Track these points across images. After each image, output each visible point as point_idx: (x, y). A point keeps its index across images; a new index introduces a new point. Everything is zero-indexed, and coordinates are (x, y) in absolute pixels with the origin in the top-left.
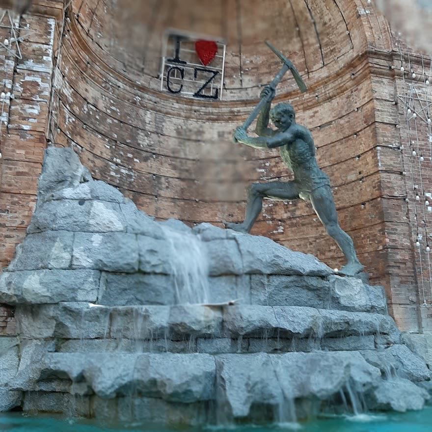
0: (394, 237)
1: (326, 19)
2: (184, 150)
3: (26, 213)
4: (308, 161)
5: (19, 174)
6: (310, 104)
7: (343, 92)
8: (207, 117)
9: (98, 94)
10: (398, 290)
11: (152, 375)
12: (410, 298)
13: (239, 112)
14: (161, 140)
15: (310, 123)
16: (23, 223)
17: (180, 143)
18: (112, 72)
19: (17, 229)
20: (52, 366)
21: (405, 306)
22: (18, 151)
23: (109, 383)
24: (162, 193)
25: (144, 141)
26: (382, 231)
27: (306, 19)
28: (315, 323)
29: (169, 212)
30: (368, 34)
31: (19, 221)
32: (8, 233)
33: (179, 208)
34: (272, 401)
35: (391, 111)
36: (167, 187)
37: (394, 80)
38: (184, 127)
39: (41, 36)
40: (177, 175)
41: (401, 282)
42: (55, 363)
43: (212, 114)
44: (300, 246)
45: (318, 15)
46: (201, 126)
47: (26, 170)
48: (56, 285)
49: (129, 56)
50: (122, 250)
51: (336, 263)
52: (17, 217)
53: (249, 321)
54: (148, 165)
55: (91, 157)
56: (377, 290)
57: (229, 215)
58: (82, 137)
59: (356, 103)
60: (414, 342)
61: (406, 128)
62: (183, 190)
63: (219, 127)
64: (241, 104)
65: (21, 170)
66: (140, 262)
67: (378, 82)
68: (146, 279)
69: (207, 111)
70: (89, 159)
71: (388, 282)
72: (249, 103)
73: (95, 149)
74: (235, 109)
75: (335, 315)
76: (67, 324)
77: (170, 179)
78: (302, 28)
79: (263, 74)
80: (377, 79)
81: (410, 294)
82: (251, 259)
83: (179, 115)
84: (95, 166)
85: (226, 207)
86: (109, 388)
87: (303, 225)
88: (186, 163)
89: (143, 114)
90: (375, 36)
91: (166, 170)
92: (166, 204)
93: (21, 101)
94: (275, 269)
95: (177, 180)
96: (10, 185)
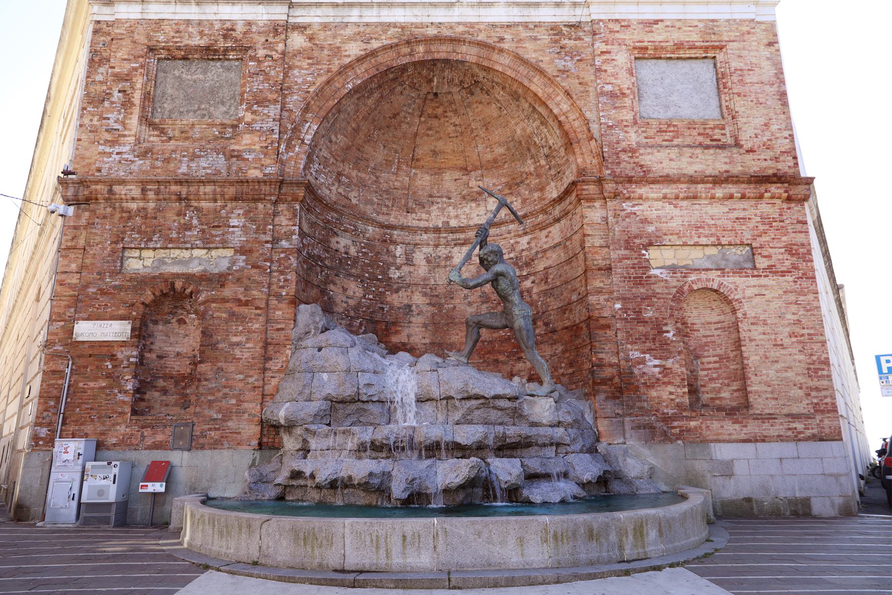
0: (601, 356)
1: (551, 142)
2: (434, 278)
4: (510, 295)
5: (278, 330)
6: (544, 224)
7: (567, 214)
9: (349, 242)
12: (617, 411)
14: (412, 270)
15: (546, 243)
16: (282, 366)
17: (430, 270)
19: (279, 371)
20: (296, 468)
22: (277, 313)
23: (324, 478)
24: (413, 319)
25: (394, 274)
27: (535, 143)
31: (280, 365)
32: (272, 375)
34: (428, 492)
35: (602, 234)
36: (418, 314)
38: (433, 255)
39: (290, 219)
40: (428, 301)
41: (607, 398)
43: (459, 239)
45: (544, 140)
46: (450, 252)
47: (282, 326)
55: (344, 299)
58: (335, 284)
61: (617, 249)
62: (433, 315)
65: (279, 326)
67: (589, 207)
68: (365, 406)
78: (533, 150)
79: (505, 195)
80: (588, 204)
82: (446, 387)
83: (428, 244)
84: (348, 306)
88: (436, 288)
89: (393, 250)
91: (418, 299)
92: (417, 329)
94: (466, 395)
96: (272, 339)
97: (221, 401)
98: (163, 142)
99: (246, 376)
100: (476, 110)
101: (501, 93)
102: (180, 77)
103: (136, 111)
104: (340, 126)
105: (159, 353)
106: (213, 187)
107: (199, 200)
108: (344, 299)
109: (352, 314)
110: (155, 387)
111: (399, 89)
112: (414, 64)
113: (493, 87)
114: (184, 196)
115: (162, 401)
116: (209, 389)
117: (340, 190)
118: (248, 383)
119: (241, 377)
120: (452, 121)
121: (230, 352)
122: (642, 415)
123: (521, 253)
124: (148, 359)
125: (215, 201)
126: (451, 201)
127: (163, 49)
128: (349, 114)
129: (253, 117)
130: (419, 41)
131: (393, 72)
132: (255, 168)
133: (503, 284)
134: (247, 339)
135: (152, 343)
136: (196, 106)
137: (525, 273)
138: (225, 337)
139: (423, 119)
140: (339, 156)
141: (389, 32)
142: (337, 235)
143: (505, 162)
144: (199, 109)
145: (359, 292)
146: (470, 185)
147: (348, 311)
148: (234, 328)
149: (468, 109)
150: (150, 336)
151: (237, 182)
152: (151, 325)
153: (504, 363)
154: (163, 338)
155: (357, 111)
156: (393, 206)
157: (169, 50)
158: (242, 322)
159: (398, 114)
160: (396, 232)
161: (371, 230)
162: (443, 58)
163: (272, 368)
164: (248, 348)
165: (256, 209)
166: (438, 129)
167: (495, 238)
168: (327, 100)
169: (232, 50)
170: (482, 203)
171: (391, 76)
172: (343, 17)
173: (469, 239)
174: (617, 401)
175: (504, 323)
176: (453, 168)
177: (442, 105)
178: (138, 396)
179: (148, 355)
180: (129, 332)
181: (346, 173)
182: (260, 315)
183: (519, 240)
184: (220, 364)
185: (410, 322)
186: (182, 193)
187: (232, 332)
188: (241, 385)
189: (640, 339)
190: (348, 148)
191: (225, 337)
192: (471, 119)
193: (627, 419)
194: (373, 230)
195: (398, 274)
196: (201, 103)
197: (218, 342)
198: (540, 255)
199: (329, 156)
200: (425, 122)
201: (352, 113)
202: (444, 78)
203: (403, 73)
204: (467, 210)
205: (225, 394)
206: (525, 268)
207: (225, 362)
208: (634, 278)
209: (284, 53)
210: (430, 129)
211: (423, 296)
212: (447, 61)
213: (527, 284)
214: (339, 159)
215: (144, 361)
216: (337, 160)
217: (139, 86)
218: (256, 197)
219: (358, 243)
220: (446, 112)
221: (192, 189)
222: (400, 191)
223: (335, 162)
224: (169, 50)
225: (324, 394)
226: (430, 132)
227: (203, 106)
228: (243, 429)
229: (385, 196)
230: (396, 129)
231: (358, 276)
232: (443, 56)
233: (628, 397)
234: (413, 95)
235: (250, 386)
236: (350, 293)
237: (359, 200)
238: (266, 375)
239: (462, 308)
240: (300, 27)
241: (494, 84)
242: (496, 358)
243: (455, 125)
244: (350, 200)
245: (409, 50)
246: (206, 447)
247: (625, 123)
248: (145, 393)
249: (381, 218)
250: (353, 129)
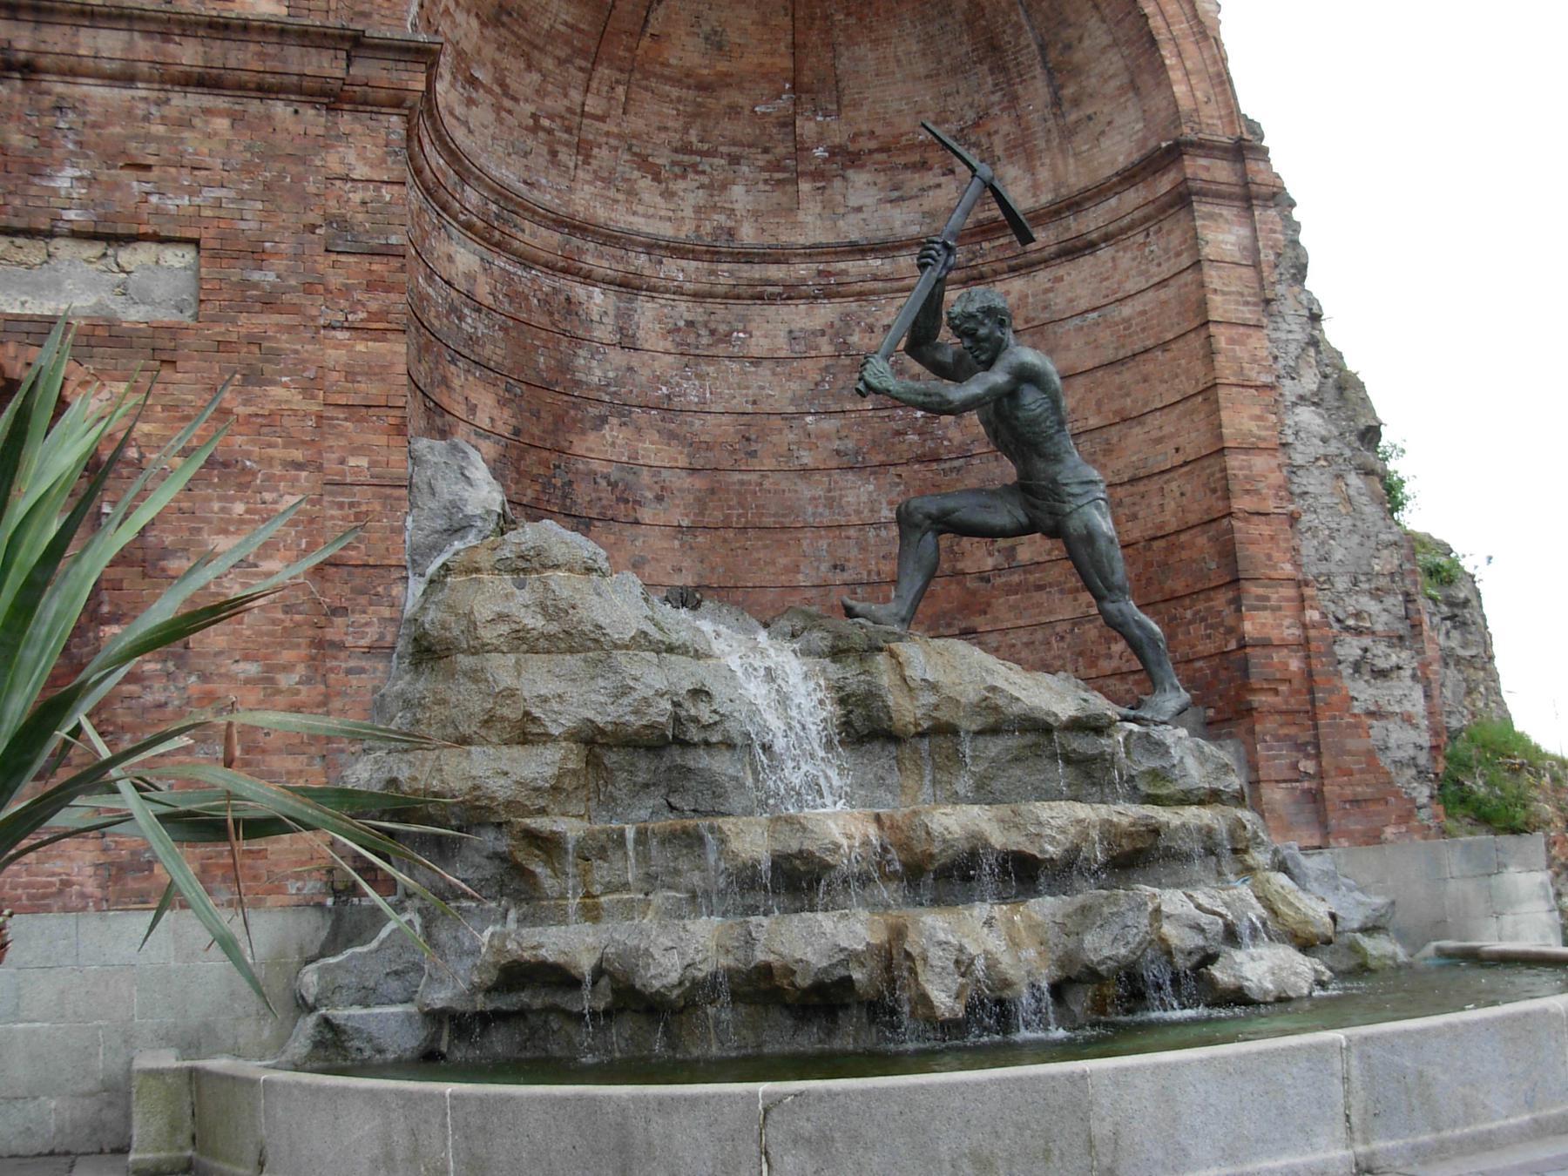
3: (386, 612)
11: (761, 956)
13: (844, 272)
16: (382, 637)
19: (371, 650)
20: (527, 955)
21: (1289, 785)
22: (352, 462)
24: (646, 514)
26: (1236, 602)
28: (1085, 836)
29: (669, 568)
30: (1180, 90)
32: (352, 663)
36: (659, 499)
37: (1250, 208)
40: (682, 461)
42: (533, 948)
44: (1032, 647)
48: (502, 782)
50: (635, 695)
51: (1127, 687)
52: (366, 624)
53: (944, 841)
56: (1224, 753)
57: (835, 567)
59: (1159, 265)
66: (677, 719)
71: (1252, 732)
72: (872, 250)
75: (1126, 813)
76: (532, 867)
77: (665, 474)
82: (933, 699)
86: (674, 986)
87: (1040, 588)
89: (583, 298)
90: (1199, 94)
93: (346, 335)
95: (684, 474)
99: (270, 669)
106: (124, 35)
107: (72, 73)
114: (22, 56)
116: (145, 709)
118: (278, 692)
119: (252, 669)
138: (186, 535)
148: (216, 506)
158: (242, 487)
163: (349, 641)
175: (1023, 519)
182: (299, 466)
185: (637, 522)
186: (17, 45)
187: (208, 521)
191: (186, 535)
195: (598, 373)
218: (269, 79)
225: (568, 722)
236: (483, 420)
239: (784, 485)
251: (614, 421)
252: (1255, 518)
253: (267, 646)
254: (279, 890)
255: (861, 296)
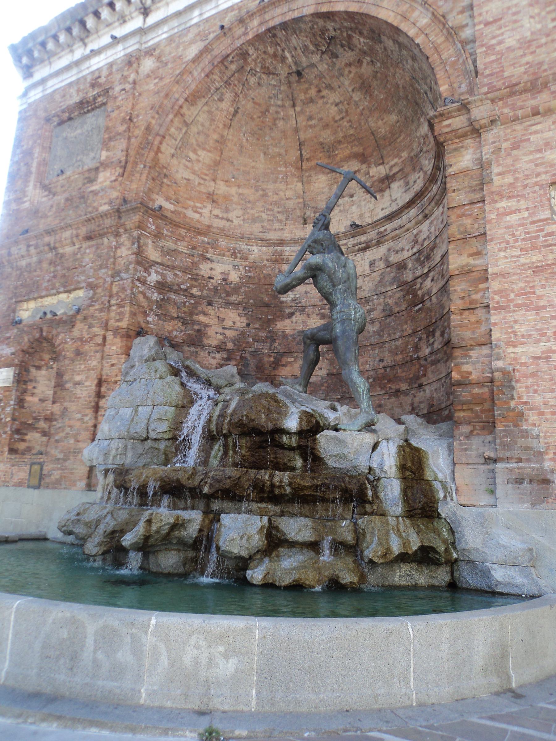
5: (113, 365)
6: (437, 197)
8: (357, 248)
9: (229, 268)
10: (466, 444)
12: (487, 454)
18: (240, 241)
21: (475, 467)
33: (327, 362)
43: (361, 243)
49: (268, 215)
54: (292, 322)
55: (220, 330)
58: (205, 314)
60: (462, 518)
63: (370, 255)
64: (386, 221)
69: (356, 242)
70: (217, 333)
72: (393, 217)
73: (225, 321)
74: (382, 229)
81: (486, 448)
84: (225, 337)
85: (377, 351)
97: (63, 441)
98: (49, 199)
100: (352, 75)
101: (362, 40)
102: (66, 138)
103: (33, 178)
104: (197, 141)
105: (41, 396)
106: (70, 231)
108: (220, 330)
109: (230, 346)
110: (36, 428)
111: (253, 80)
112: (250, 43)
113: (350, 37)
115: (42, 442)
117: (216, 212)
119: (79, 416)
120: (331, 101)
121: (72, 391)
122: (528, 460)
123: (422, 245)
124: (29, 402)
125: (74, 244)
126: (354, 199)
127: (54, 116)
128: (203, 125)
129: (109, 153)
130: (252, 15)
131: (232, 62)
132: (105, 204)
133: (324, 281)
134: (87, 377)
135: (34, 388)
136: (74, 160)
137: (426, 271)
139: (298, 109)
140: (206, 175)
141: (227, 19)
142: (212, 261)
143: (401, 132)
144: (77, 161)
145: (241, 322)
146: (371, 174)
147: (225, 343)
149: (342, 79)
150: (31, 381)
151: (86, 221)
152: (33, 371)
153: (406, 393)
154: (47, 382)
155: (213, 120)
156: (287, 219)
157: (58, 116)
158: (85, 360)
159: (267, 110)
160: (288, 248)
161: (256, 251)
162: (278, 23)
164: (86, 387)
165: (103, 244)
166: (320, 116)
167: (397, 232)
168: (167, 115)
169: (99, 96)
170: (387, 193)
171: (233, 67)
172: (185, 23)
173: (371, 241)
174: (489, 438)
176: (348, 158)
177: (311, 84)
178: (16, 436)
179: (28, 398)
180: (12, 377)
181: (220, 192)
183: (421, 227)
184: (66, 404)
187: (75, 372)
188: (78, 424)
189: (530, 336)
190: (217, 163)
192: (350, 90)
193: (500, 466)
194: (260, 251)
196: (78, 155)
197: (66, 382)
198: (438, 241)
199: (192, 177)
200: (302, 112)
201: (207, 124)
202: (296, 49)
203: (245, 60)
204: (371, 206)
205: (67, 434)
206: (426, 263)
207: (70, 401)
208: (523, 240)
209: (134, 83)
210: (310, 118)
211: (321, 319)
212: (284, 26)
213: (428, 283)
214: (207, 178)
215: (25, 405)
216: (205, 180)
217: (36, 155)
218: (101, 232)
219: (241, 268)
220: (319, 91)
221: (57, 237)
222: (292, 202)
223: (202, 182)
224: (58, 116)
226: (313, 122)
227: (79, 158)
228: (76, 469)
229: (276, 210)
230: (271, 129)
231: (239, 304)
232: (277, 21)
233: (504, 431)
234: (273, 82)
235: (84, 425)
237: (244, 220)
238: (100, 413)
240: (151, 50)
241: (350, 32)
242: (398, 387)
243: (337, 105)
244: (232, 221)
245: (243, 30)
246: (50, 486)
247: (514, 10)
248: (26, 434)
249: (273, 236)
250: (217, 141)
251: (298, 314)
252: (467, 313)
253: (83, 408)
254: (75, 485)
255: (394, 239)
